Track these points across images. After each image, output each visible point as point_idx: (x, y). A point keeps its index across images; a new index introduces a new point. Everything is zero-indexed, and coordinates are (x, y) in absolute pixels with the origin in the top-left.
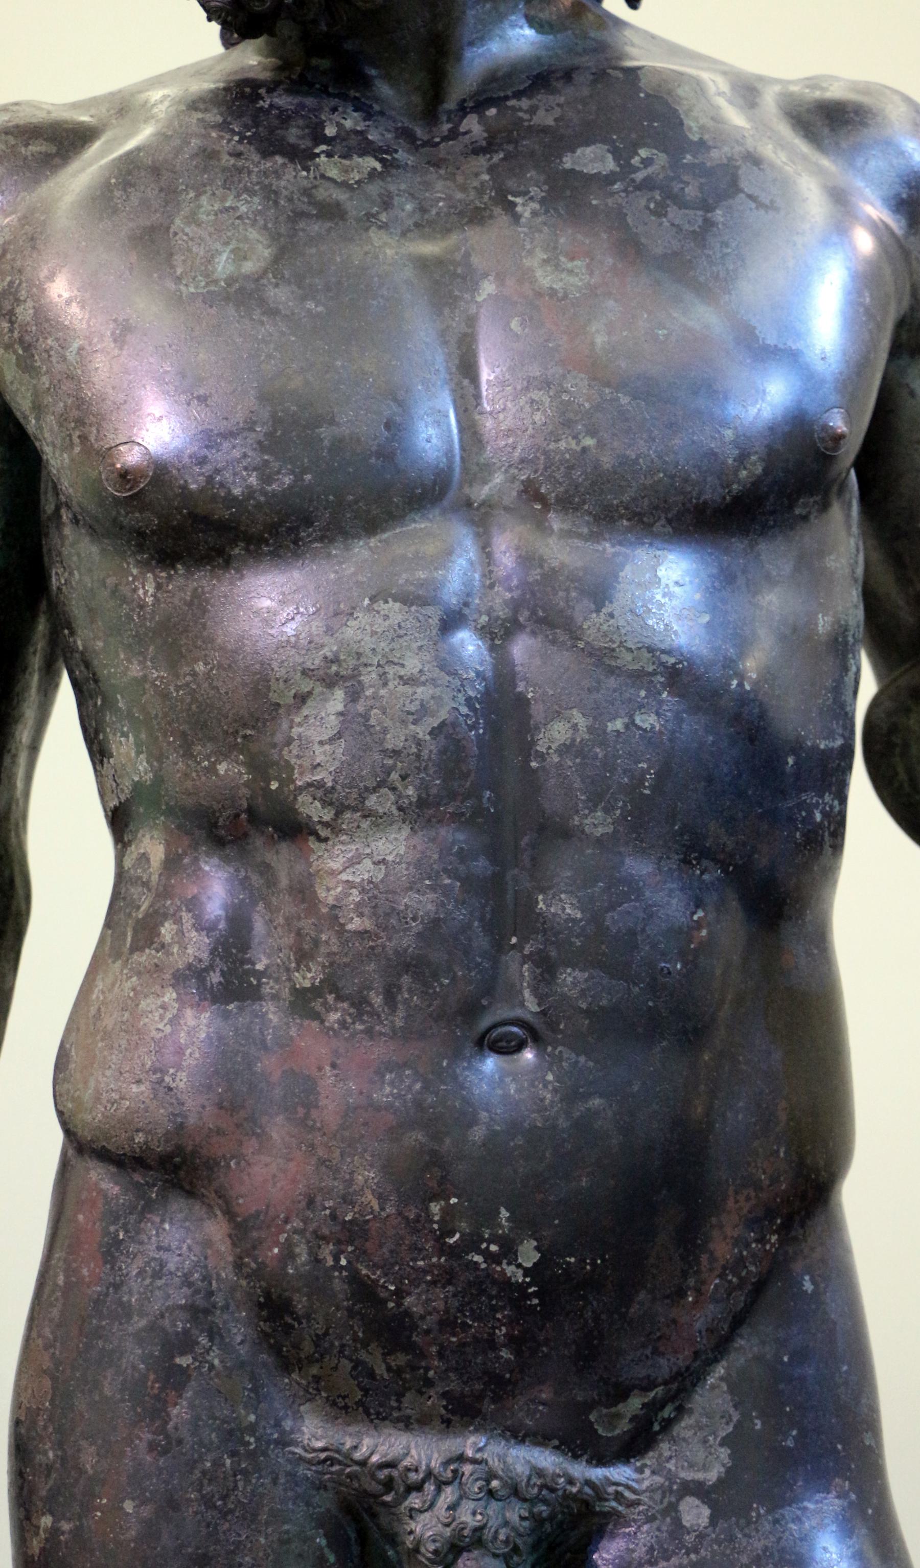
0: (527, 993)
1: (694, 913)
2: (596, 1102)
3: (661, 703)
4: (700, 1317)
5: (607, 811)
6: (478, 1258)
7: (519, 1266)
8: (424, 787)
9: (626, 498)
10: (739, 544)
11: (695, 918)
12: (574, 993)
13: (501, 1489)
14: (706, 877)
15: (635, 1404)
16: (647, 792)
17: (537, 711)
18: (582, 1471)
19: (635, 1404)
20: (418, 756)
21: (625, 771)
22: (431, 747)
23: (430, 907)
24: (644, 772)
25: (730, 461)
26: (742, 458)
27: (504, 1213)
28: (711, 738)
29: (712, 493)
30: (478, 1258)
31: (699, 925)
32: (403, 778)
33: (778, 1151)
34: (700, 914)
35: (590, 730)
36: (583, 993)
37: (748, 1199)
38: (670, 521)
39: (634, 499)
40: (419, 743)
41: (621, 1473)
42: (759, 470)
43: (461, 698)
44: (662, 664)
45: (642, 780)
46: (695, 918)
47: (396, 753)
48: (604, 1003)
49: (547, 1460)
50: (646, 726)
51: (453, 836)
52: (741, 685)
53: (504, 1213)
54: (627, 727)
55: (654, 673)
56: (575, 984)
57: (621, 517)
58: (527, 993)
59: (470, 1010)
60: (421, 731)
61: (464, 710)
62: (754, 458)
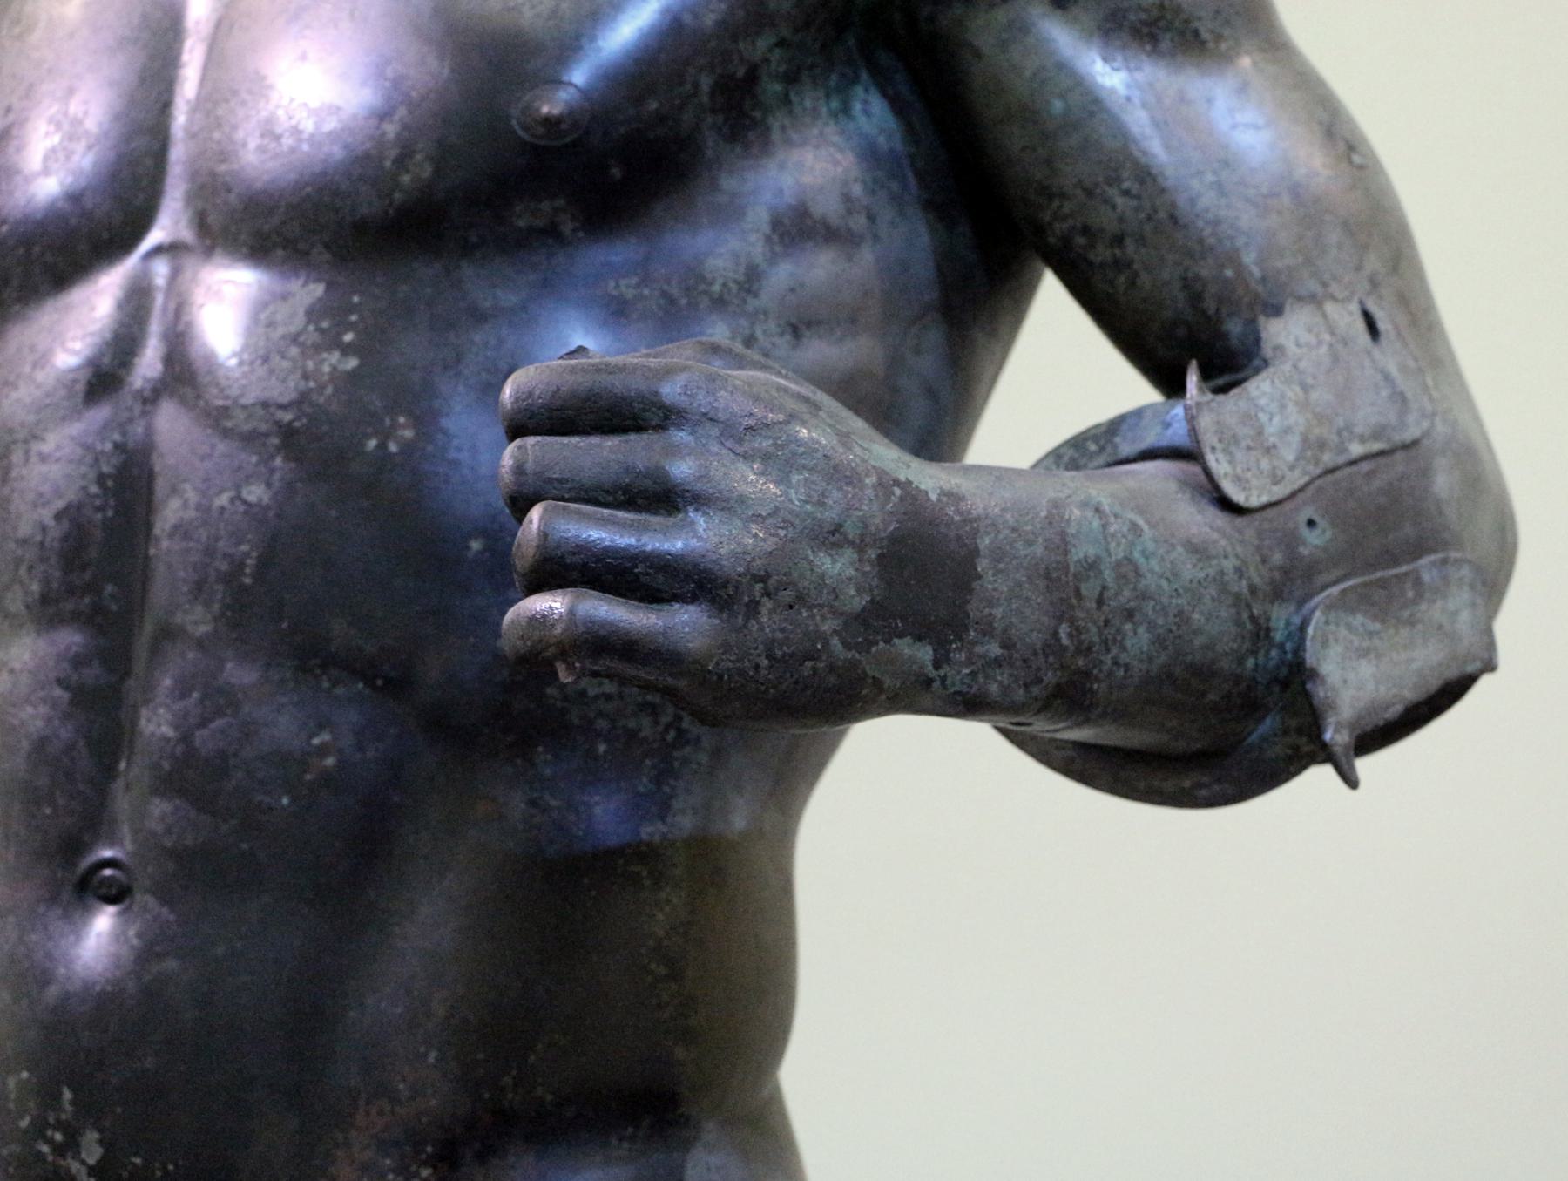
0: (125, 829)
1: (314, 735)
2: (171, 964)
3: (272, 471)
5: (207, 605)
6: (45, 1149)
7: (83, 1163)
8: (46, 581)
9: (276, 220)
10: (427, 270)
11: (316, 741)
12: (160, 828)
14: (340, 691)
16: (247, 581)
17: (161, 486)
20: (42, 544)
21: (225, 555)
22: (56, 532)
23: (39, 723)
24: (247, 555)
25: (388, 164)
26: (402, 161)
27: (67, 1095)
28: (333, 513)
29: (369, 205)
30: (45, 1149)
31: (322, 751)
32: (30, 568)
33: (426, 1055)
34: (326, 737)
35: (198, 507)
36: (168, 831)
37: (381, 1113)
38: (327, 246)
39: (284, 223)
40: (44, 529)
42: (427, 171)
43: (92, 475)
44: (278, 424)
45: (242, 565)
46: (316, 741)
47: (24, 542)
48: (189, 842)
50: (252, 498)
51: (71, 639)
52: (382, 446)
53: (67, 1095)
54: (232, 501)
55: (267, 435)
56: (162, 818)
57: (275, 245)
58: (125, 829)
59: (73, 847)
60: (47, 515)
61: (94, 489)
62: (418, 157)
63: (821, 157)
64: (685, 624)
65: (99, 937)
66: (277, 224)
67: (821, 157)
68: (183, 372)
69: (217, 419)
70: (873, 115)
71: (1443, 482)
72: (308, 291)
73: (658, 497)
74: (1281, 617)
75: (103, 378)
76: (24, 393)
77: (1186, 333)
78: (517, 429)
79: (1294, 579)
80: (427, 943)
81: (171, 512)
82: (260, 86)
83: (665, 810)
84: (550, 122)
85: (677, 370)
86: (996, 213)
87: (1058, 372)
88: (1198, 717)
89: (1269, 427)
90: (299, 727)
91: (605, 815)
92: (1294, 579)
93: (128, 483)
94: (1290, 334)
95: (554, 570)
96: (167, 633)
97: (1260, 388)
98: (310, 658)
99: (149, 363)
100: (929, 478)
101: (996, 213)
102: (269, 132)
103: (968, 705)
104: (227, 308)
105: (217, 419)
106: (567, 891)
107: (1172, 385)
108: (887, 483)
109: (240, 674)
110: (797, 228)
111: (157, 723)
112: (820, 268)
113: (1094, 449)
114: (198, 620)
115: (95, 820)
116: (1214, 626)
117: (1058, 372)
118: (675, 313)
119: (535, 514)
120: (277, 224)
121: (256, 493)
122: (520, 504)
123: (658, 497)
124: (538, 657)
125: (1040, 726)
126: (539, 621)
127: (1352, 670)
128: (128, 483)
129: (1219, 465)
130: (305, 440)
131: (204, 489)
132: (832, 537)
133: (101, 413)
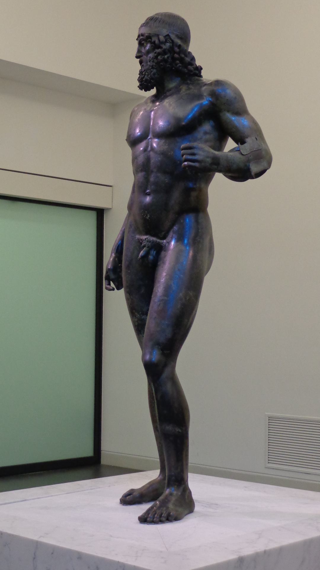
4: (167, 224)
13: (149, 241)
15: (163, 233)
18: (158, 240)
19: (163, 233)
41: (162, 241)
49: (154, 239)
59: (145, 191)
63: (207, 126)
64: (197, 164)
65: (148, 199)
66: (160, 135)
67: (207, 126)
68: (153, 149)
69: (156, 152)
70: (212, 123)
71: (263, 153)
72: (163, 141)
73: (194, 154)
74: (247, 164)
75: (145, 150)
76: (138, 152)
77: (240, 140)
78: (182, 149)
79: (249, 161)
80: (176, 195)
81: (152, 161)
82: (158, 123)
83: (195, 184)
84: (183, 125)
85: (195, 144)
86: (223, 132)
87: (230, 144)
88: (240, 173)
89: (246, 148)
90: (165, 179)
91: (191, 185)
92: (249, 161)
93: (148, 159)
94: (248, 140)
95: (186, 160)
96: (152, 172)
97: (245, 145)
98: (165, 172)
99: (149, 149)
100: (217, 153)
101: (223, 132)
102: (159, 127)
103: (220, 171)
104: (155, 143)
105: (156, 152)
106: (187, 191)
107: (238, 144)
108: (212, 153)
109: (159, 175)
110: (206, 133)
111: (152, 179)
112: (208, 137)
113: (231, 151)
114: (155, 170)
115: (147, 189)
116: (242, 165)
117: (230, 144)
118: (195, 141)
119: (184, 156)
120: (160, 135)
121: (159, 159)
122: (183, 156)
123: (194, 154)
124: (185, 167)
125: (227, 174)
126: (185, 165)
127: (254, 169)
128: (148, 159)
129: (242, 151)
130: (163, 154)
131: (155, 159)
132: (208, 157)
133: (146, 153)
